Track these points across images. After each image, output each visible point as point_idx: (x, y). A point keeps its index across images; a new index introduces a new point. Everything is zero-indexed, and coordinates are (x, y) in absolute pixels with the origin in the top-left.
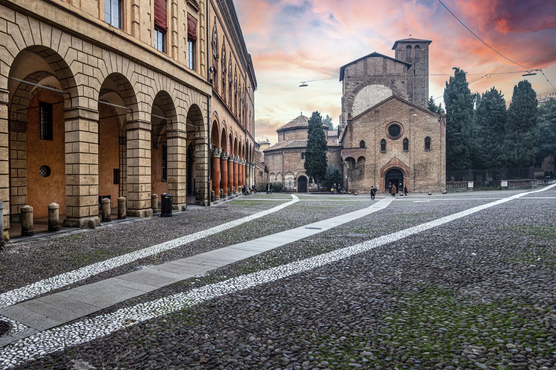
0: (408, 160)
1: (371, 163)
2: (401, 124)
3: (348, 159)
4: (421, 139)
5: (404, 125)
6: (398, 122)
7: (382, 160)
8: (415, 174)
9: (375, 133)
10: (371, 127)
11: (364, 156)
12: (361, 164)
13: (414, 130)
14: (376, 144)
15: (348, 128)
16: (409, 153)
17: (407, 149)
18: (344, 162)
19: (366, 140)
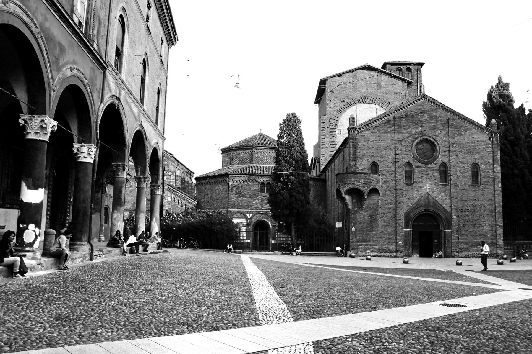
0: (448, 200)
1: (389, 201)
2: (435, 140)
3: (350, 192)
4: (466, 166)
5: (440, 142)
6: (430, 137)
7: (405, 199)
8: (459, 224)
9: (395, 151)
10: (389, 141)
11: (377, 187)
12: (372, 202)
13: (455, 151)
14: (397, 170)
15: (350, 141)
16: (448, 187)
17: (446, 182)
18: (344, 195)
19: (381, 162)
